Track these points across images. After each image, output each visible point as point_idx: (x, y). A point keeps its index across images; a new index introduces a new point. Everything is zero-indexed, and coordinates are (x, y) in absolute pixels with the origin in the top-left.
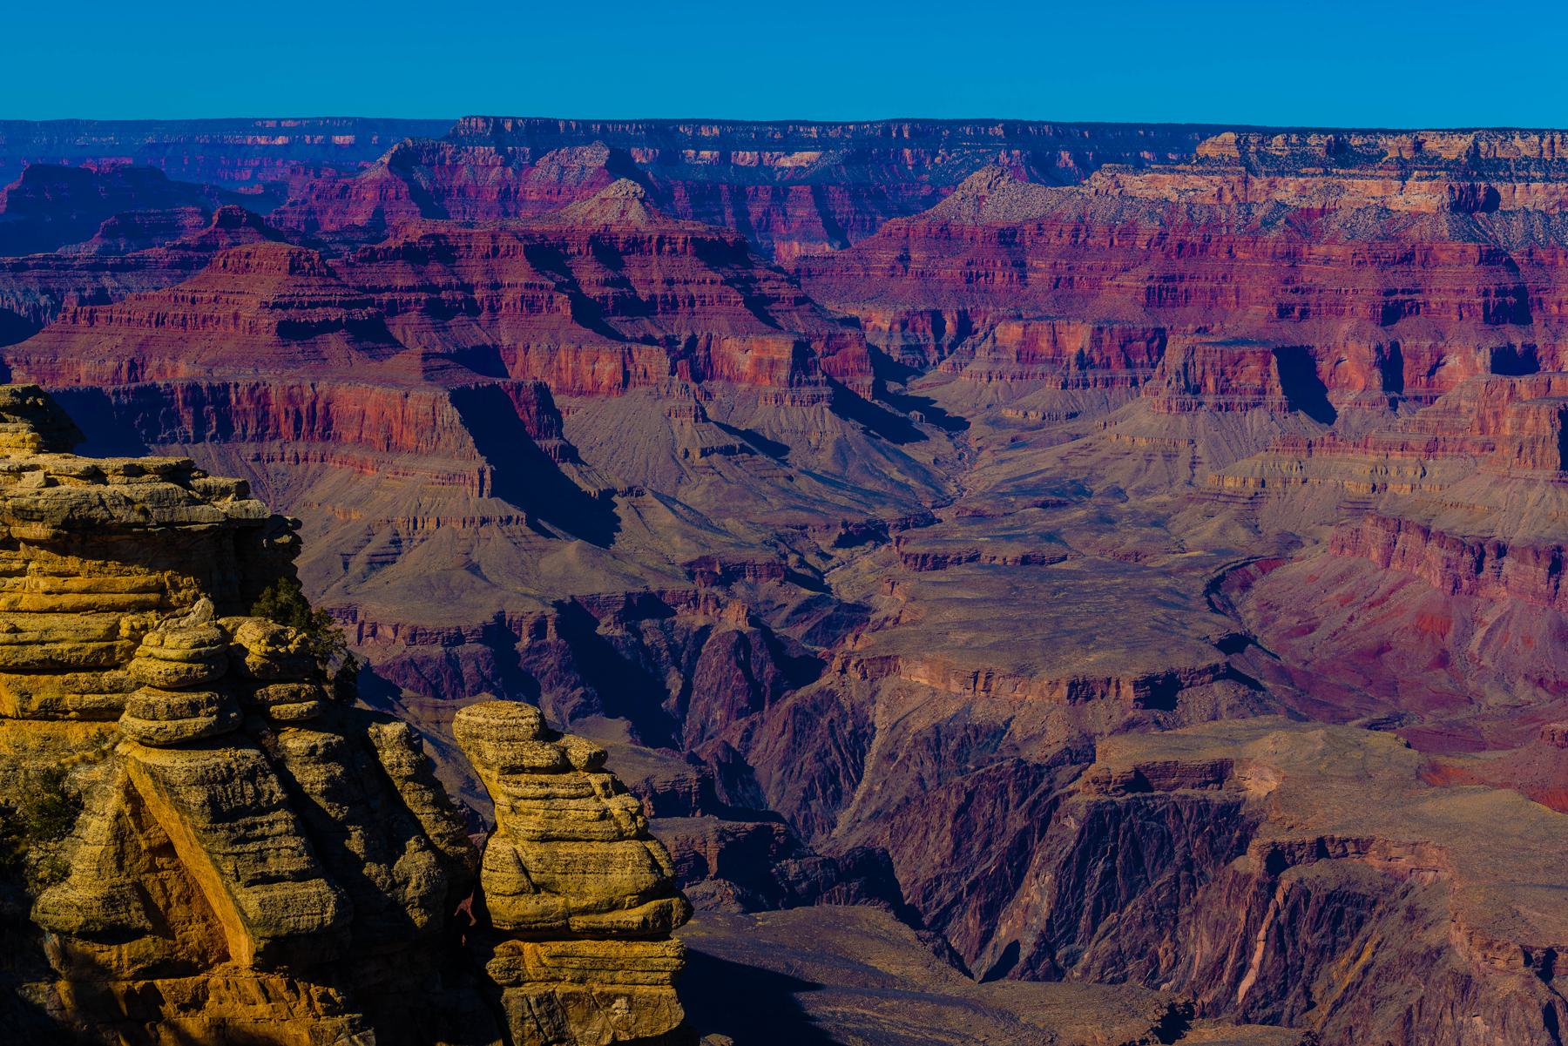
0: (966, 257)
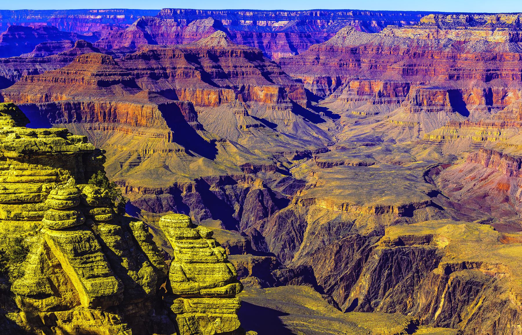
0: (340, 58)
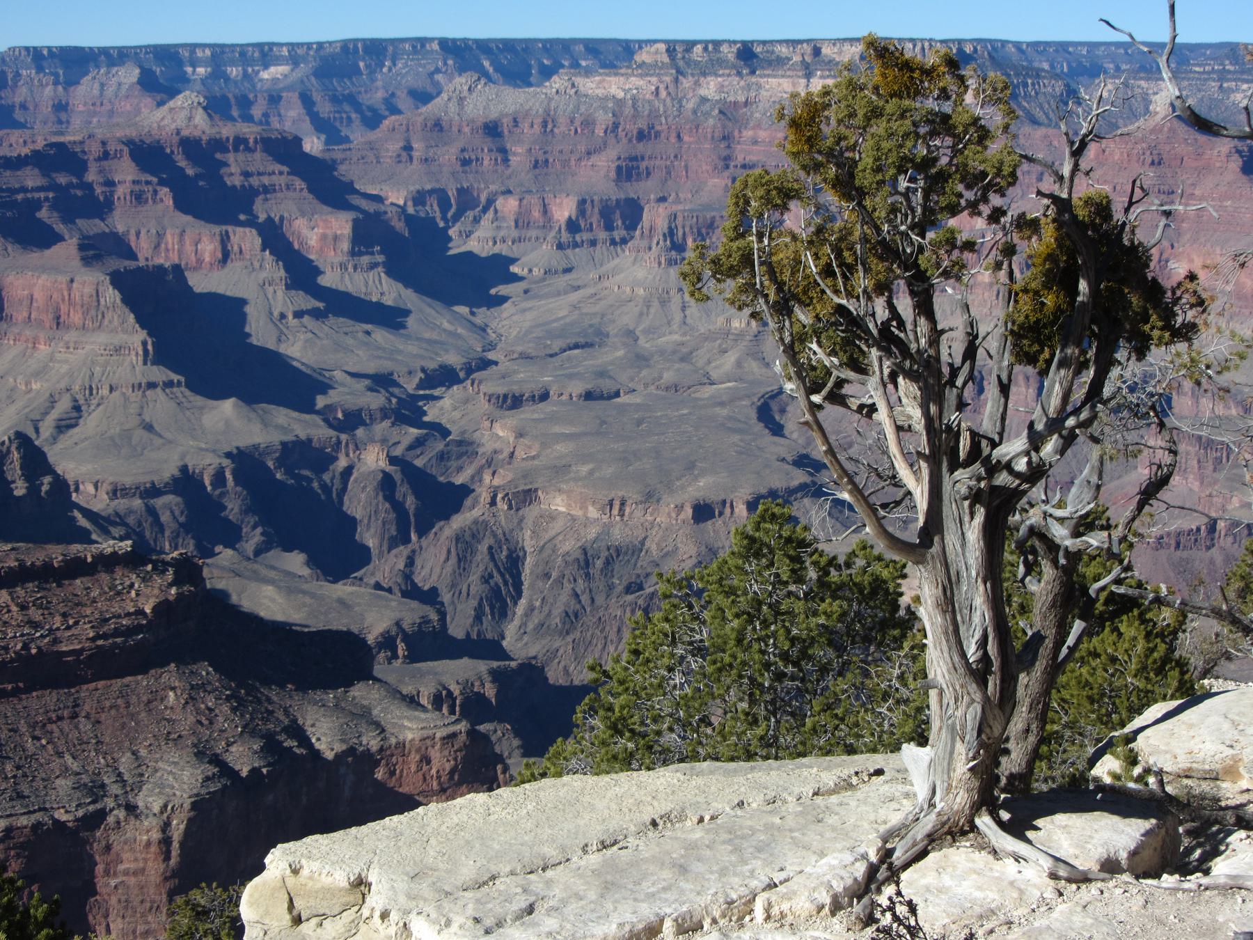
0: (460, 145)
